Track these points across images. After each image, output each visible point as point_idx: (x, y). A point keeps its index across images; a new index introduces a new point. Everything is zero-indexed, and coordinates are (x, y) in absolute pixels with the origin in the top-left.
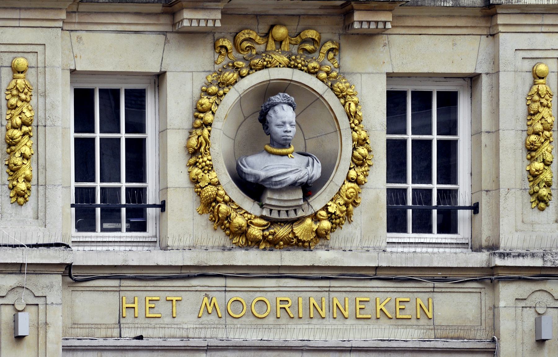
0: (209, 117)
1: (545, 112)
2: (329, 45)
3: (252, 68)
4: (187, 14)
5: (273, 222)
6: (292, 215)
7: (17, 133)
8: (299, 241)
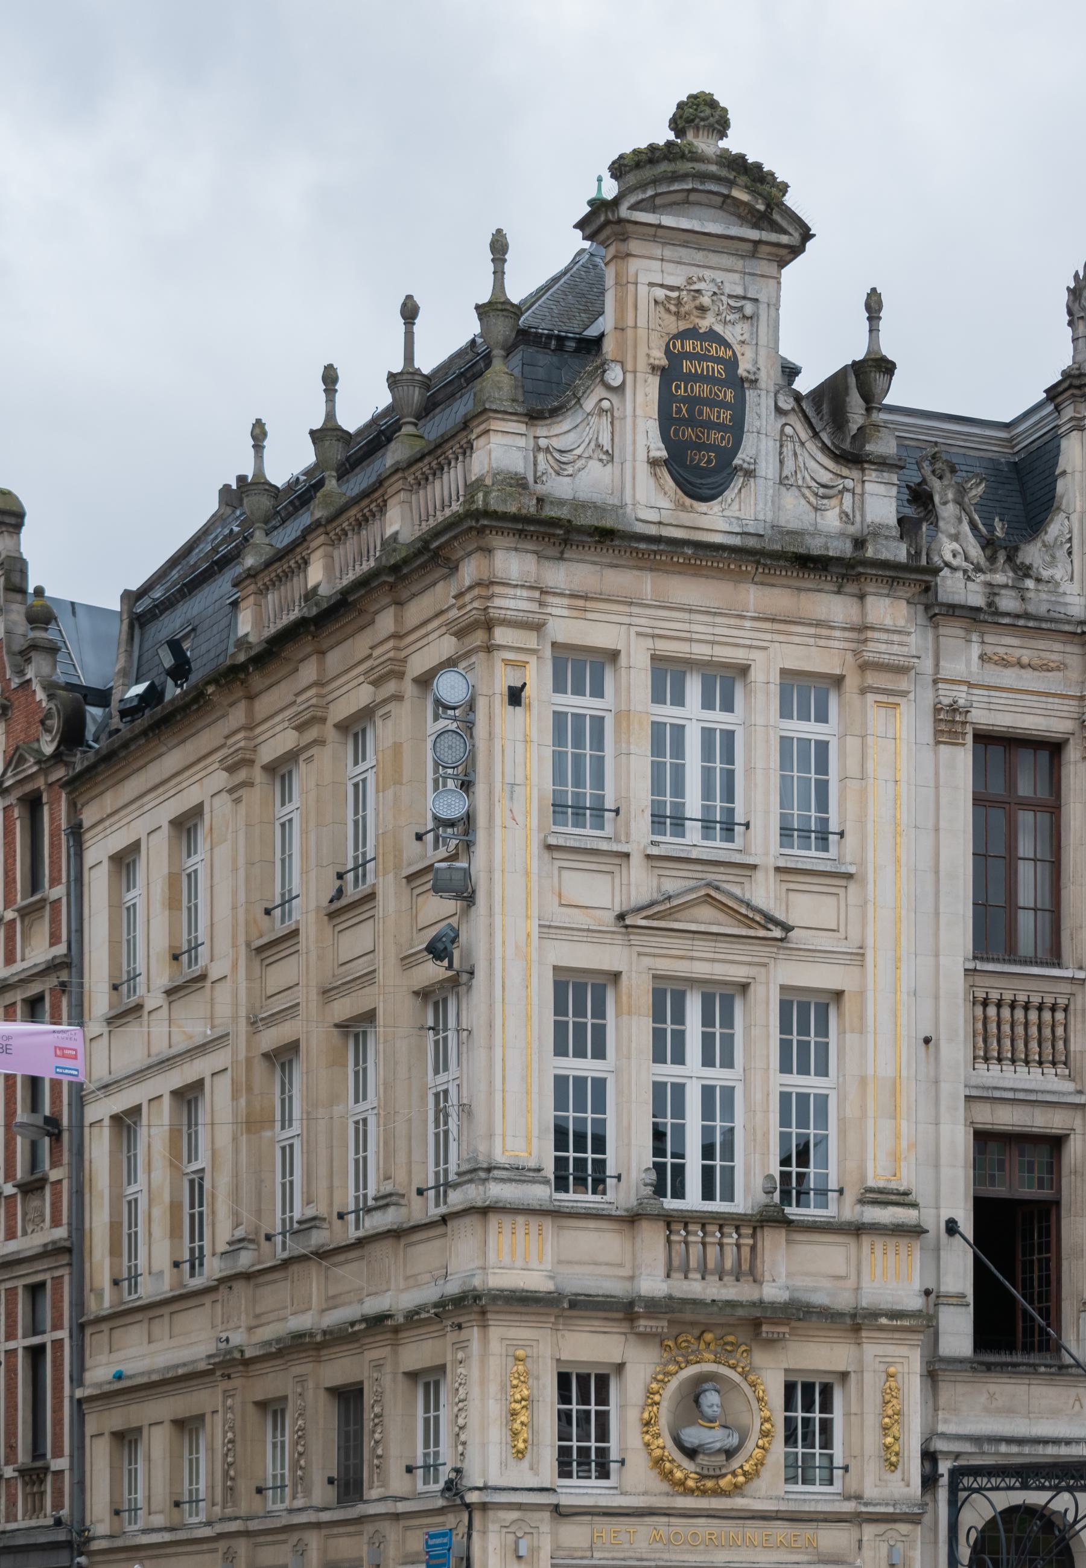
0: (657, 1398)
1: (894, 1401)
2: (743, 1348)
3: (688, 1363)
4: (642, 1322)
5: (703, 1477)
6: (718, 1472)
7: (518, 1406)
8: (722, 1490)
